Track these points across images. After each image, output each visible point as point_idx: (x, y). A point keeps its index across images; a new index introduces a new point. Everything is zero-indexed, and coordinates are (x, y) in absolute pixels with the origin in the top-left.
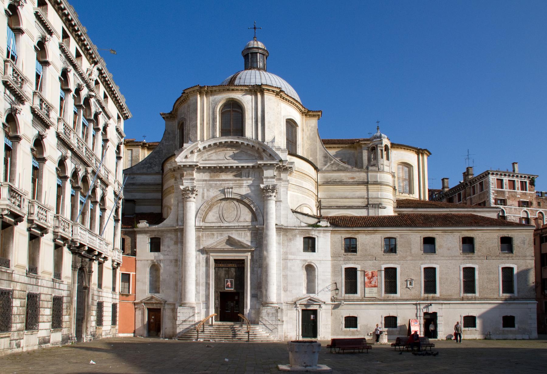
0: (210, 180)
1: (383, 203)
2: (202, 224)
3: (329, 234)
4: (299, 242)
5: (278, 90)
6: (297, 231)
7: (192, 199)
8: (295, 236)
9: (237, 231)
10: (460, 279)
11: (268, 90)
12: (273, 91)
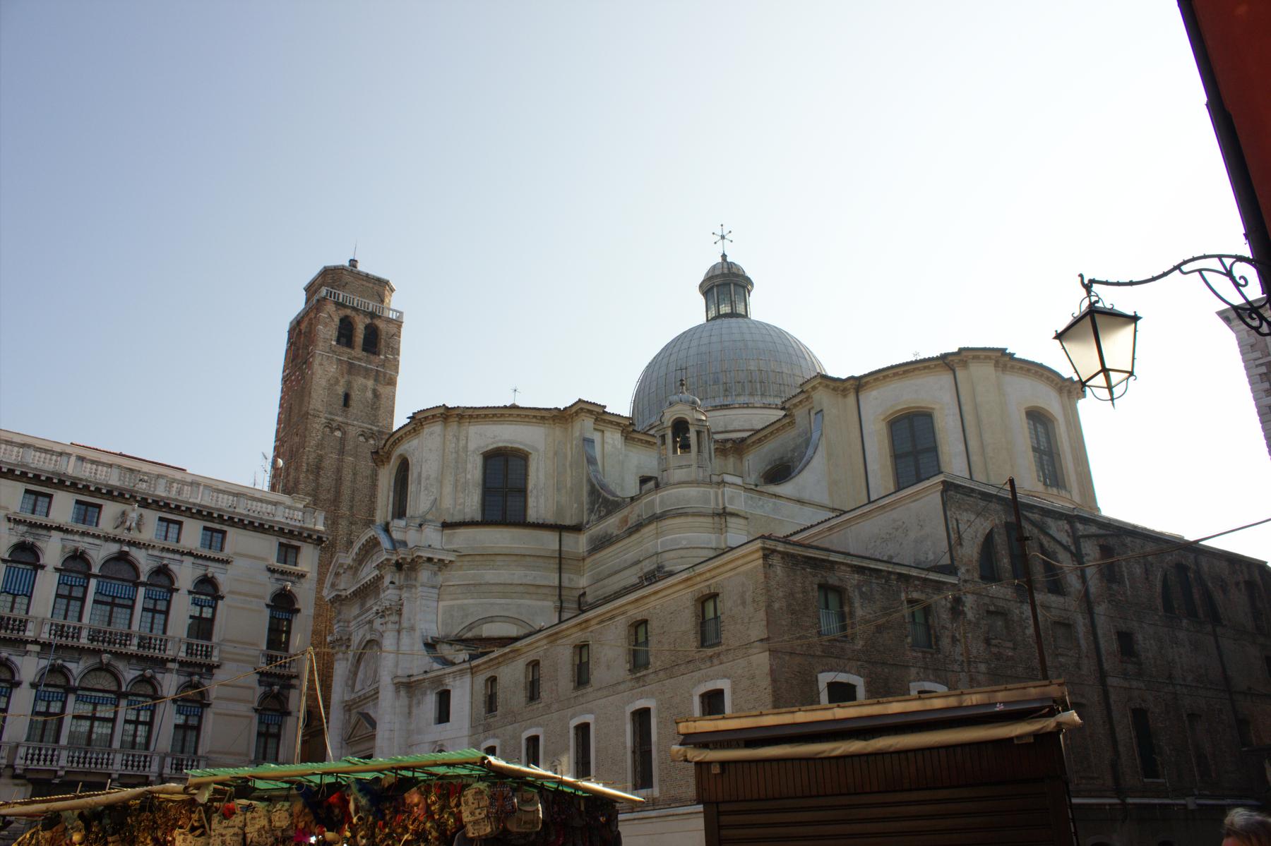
0: (359, 615)
1: (666, 563)
2: (353, 696)
3: (467, 678)
4: (430, 703)
5: (442, 411)
6: (426, 684)
7: (340, 655)
8: (424, 694)
9: (373, 700)
10: (625, 747)
11: (426, 418)
12: (434, 416)
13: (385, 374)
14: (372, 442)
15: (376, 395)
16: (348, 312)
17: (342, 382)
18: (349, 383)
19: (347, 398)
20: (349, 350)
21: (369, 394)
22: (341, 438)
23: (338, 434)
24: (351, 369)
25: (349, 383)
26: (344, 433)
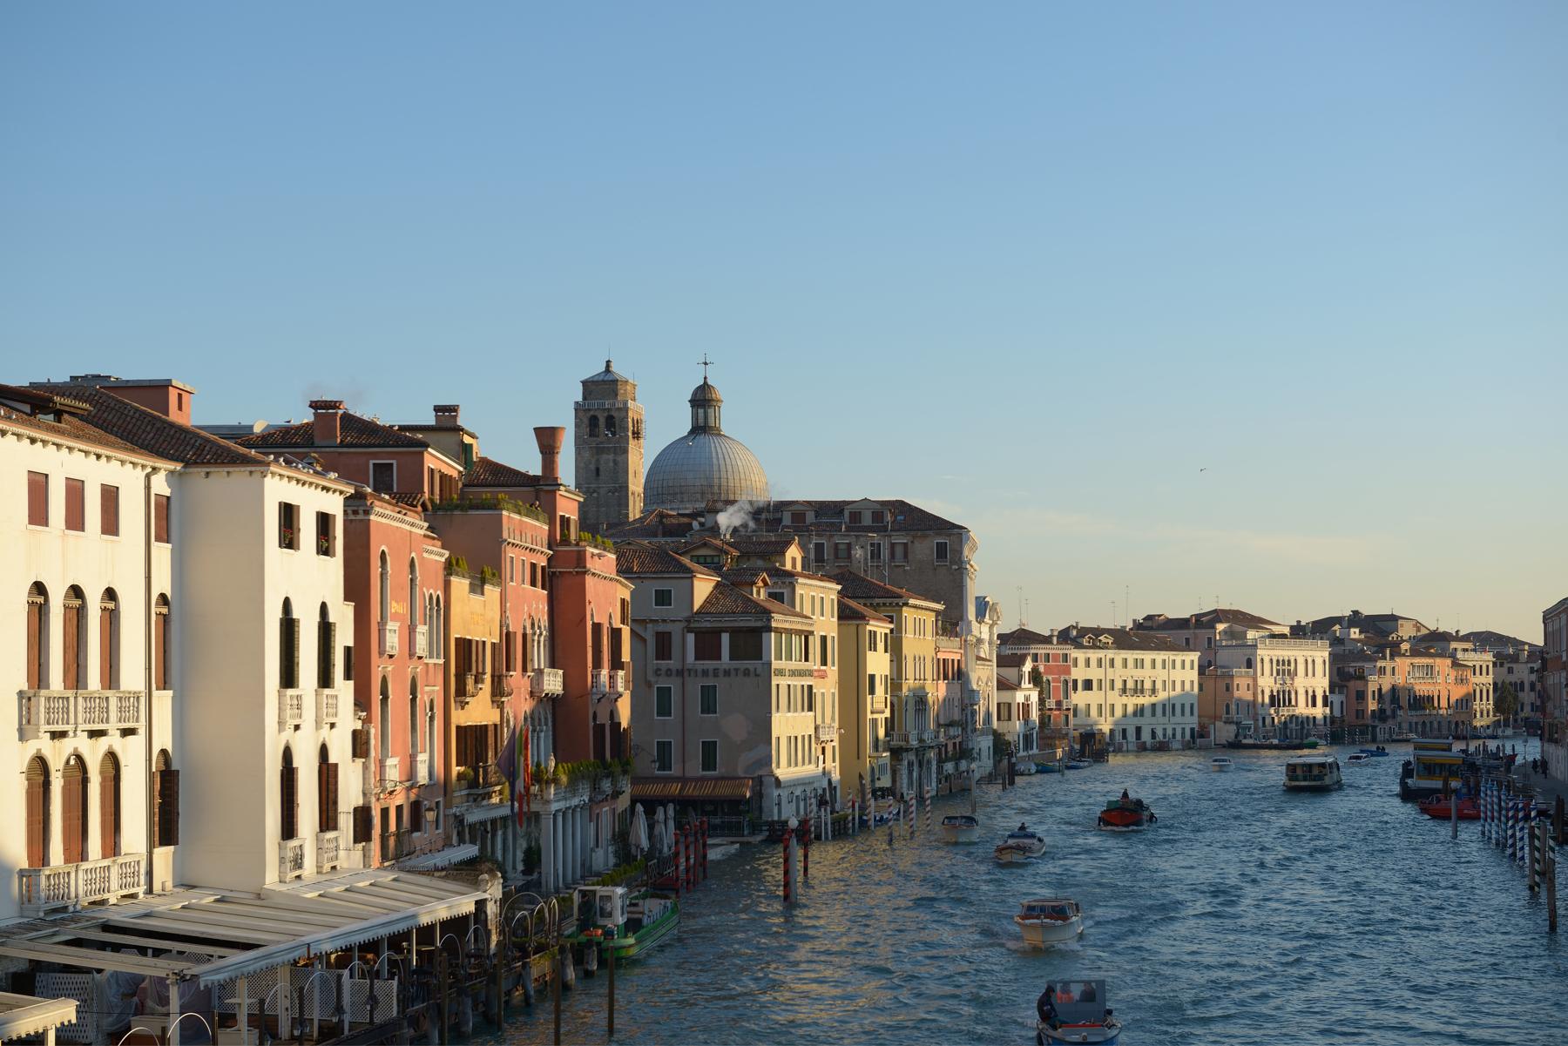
13: (620, 447)
14: (617, 494)
15: (615, 462)
16: (592, 413)
17: (593, 461)
18: (598, 460)
19: (598, 470)
20: (595, 439)
21: (611, 464)
22: (597, 498)
23: (595, 495)
24: (599, 450)
25: (598, 460)
26: (598, 493)
